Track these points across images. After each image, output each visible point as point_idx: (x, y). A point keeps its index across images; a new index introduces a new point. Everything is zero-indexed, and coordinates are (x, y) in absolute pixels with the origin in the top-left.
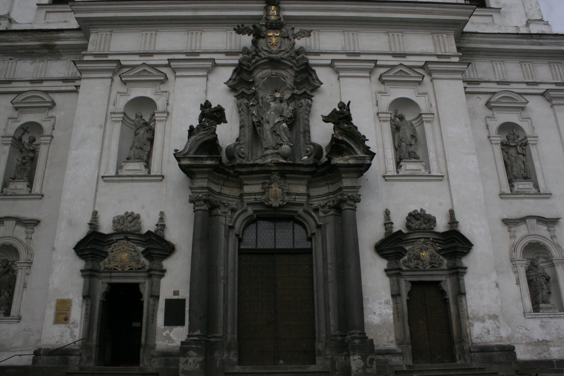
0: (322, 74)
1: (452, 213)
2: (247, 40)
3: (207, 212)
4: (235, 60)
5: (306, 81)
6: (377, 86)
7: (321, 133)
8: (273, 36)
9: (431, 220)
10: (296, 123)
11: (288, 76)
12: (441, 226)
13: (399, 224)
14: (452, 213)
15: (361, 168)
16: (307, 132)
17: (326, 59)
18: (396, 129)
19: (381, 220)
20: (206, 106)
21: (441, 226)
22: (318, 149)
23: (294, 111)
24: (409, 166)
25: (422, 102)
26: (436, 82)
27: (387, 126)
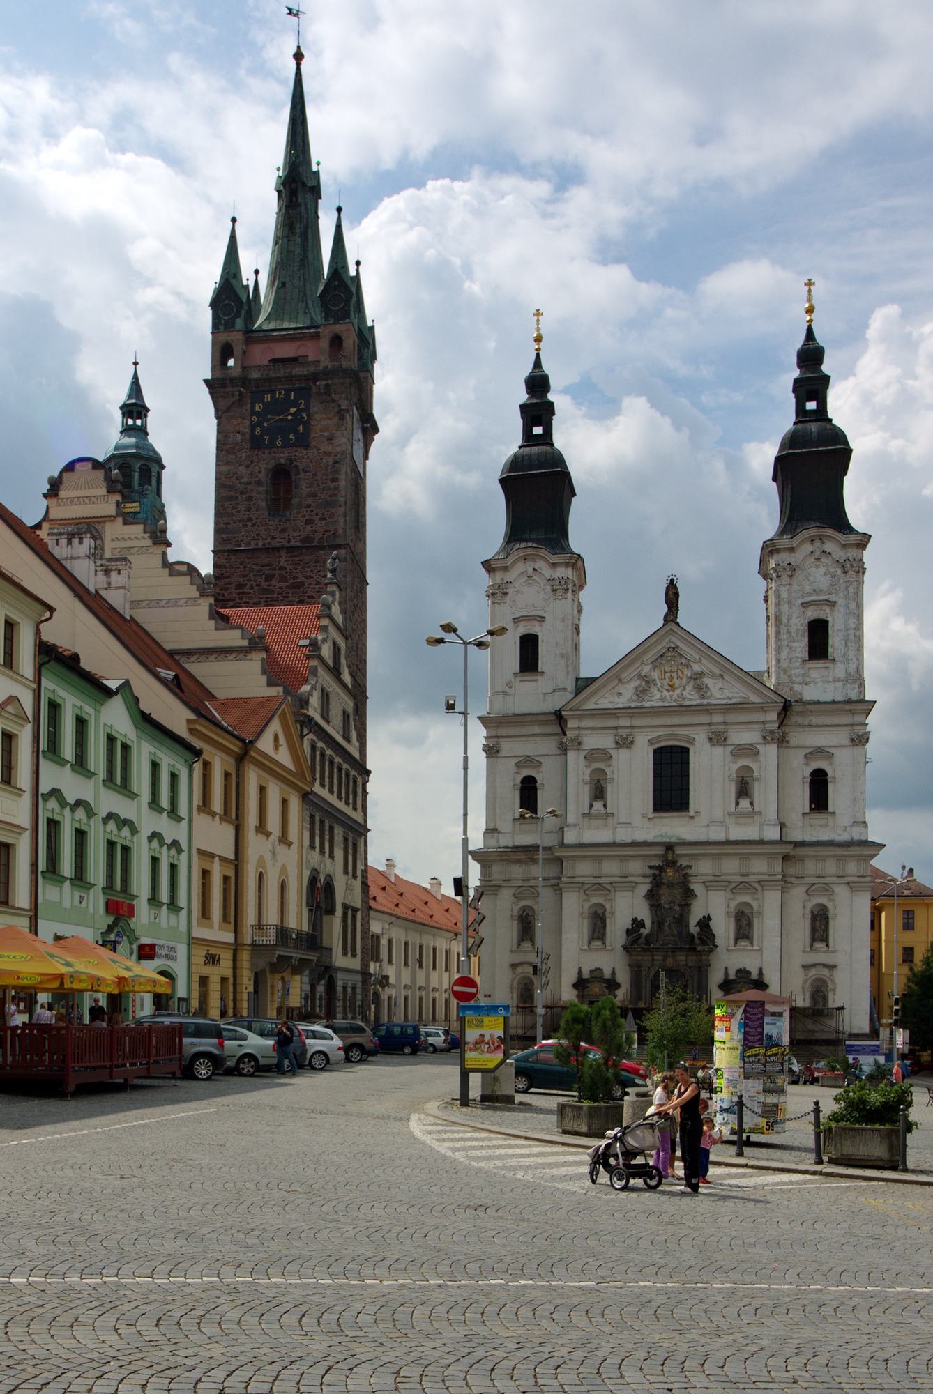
0: (696, 888)
1: (761, 969)
2: (657, 872)
3: (636, 971)
4: (648, 880)
5: (689, 894)
6: (729, 895)
7: (694, 929)
8: (670, 872)
9: (749, 973)
10: (682, 920)
11: (678, 893)
12: (754, 976)
13: (732, 976)
14: (761, 969)
15: (711, 951)
16: (687, 926)
17: (700, 879)
18: (738, 920)
19: (723, 970)
20: (635, 920)
21: (754, 976)
22: (692, 936)
23: (681, 915)
24: (743, 943)
25: (755, 904)
26: (766, 893)
27: (732, 920)
